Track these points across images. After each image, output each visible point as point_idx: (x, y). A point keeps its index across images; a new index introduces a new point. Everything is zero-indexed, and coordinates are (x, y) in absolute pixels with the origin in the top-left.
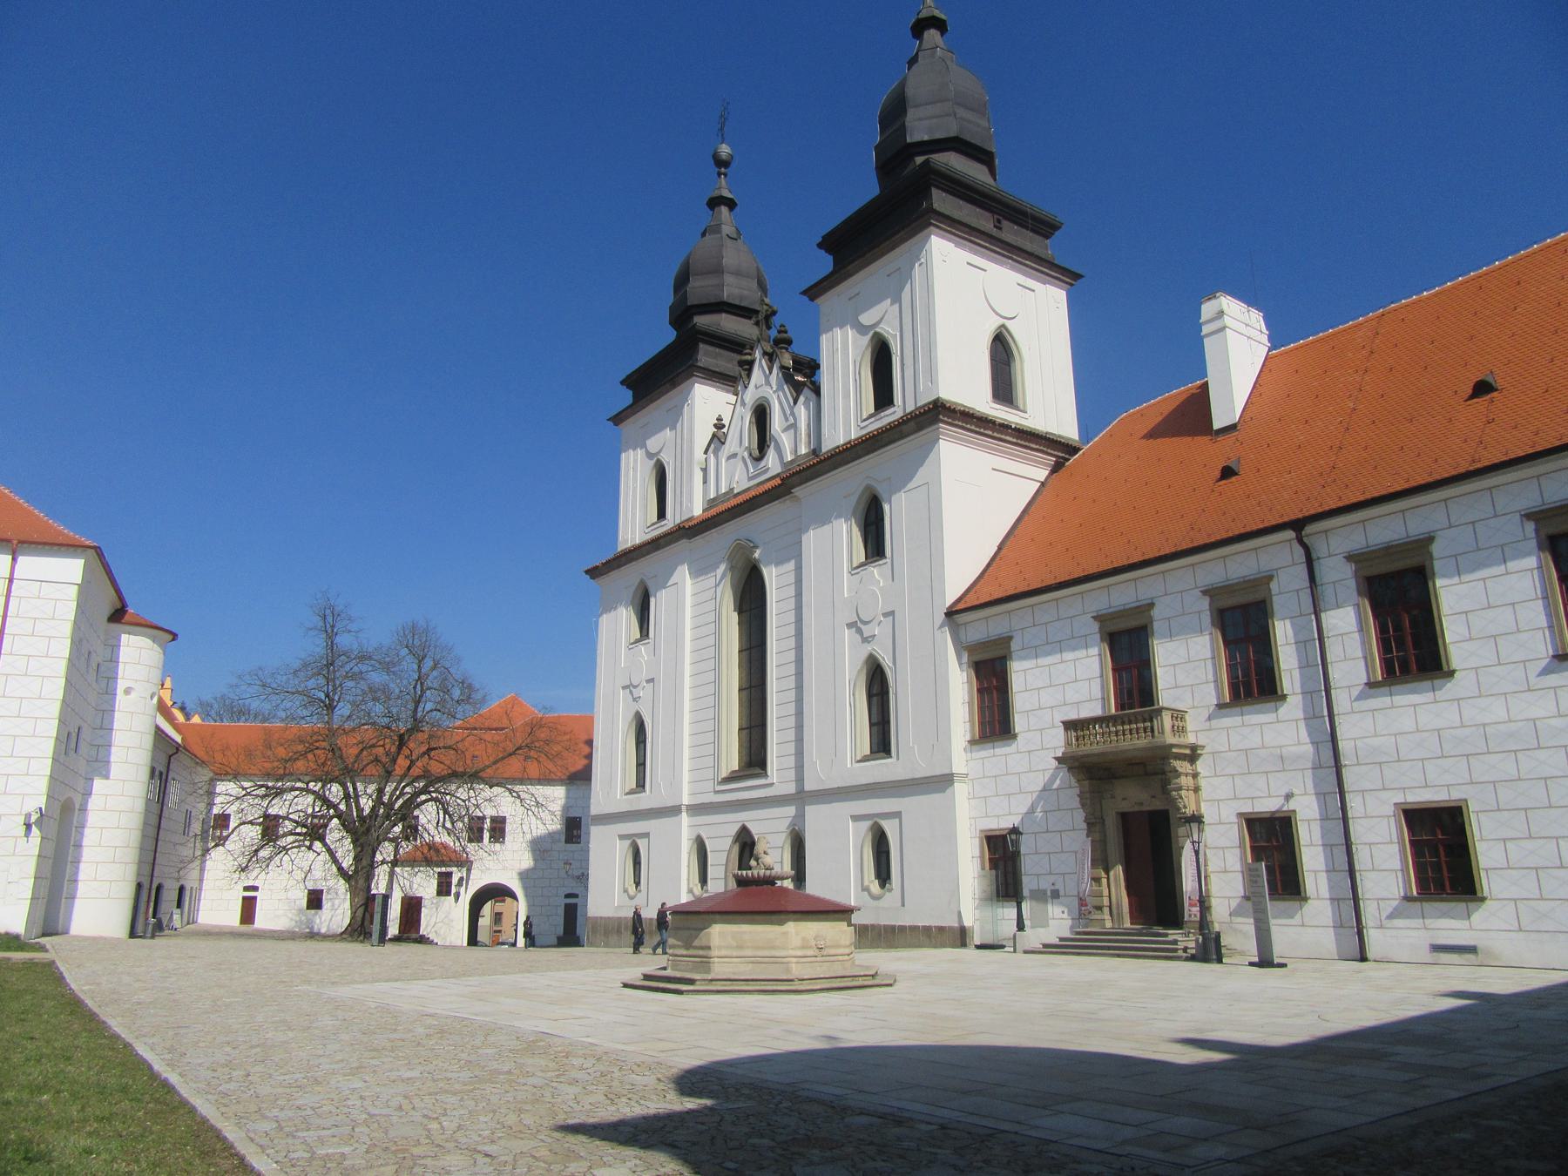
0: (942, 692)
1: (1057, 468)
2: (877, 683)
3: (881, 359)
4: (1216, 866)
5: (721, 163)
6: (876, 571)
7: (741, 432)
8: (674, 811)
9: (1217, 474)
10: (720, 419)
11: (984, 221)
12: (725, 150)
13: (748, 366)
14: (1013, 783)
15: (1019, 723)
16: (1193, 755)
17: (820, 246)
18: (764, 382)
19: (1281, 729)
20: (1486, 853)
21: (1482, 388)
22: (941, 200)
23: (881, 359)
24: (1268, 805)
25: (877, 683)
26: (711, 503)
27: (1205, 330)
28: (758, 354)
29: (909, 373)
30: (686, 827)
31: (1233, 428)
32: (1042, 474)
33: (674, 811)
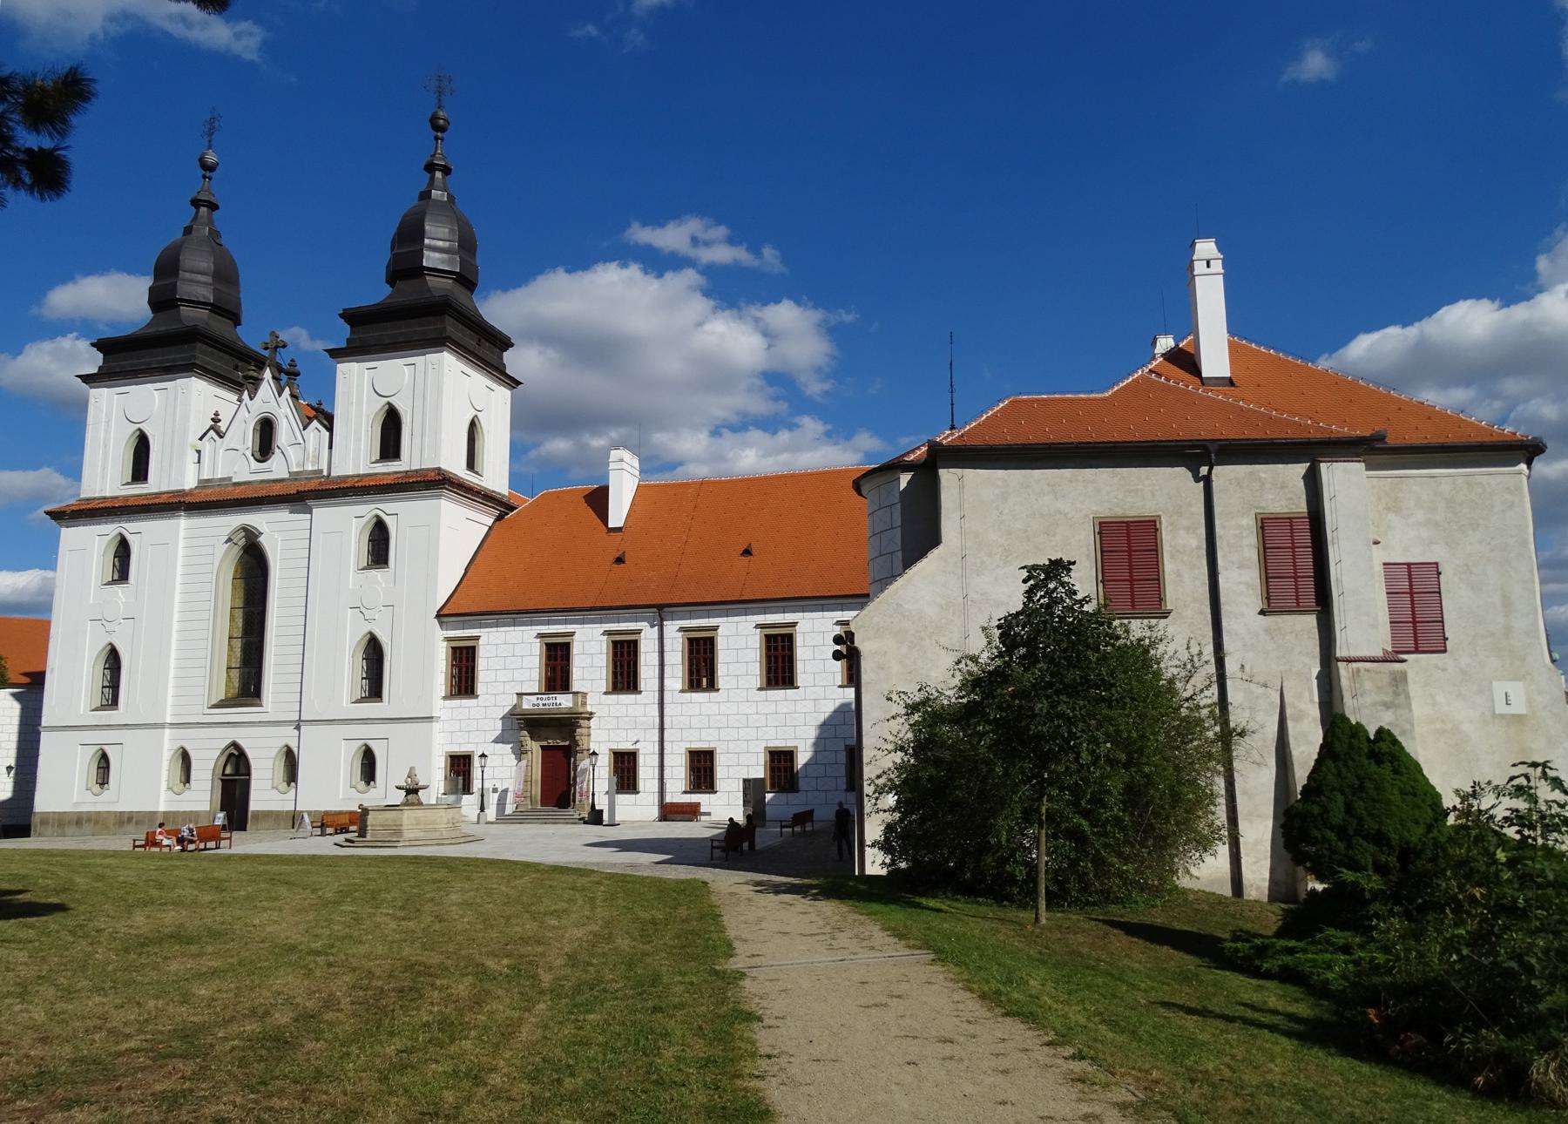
0: (420, 660)
1: (499, 518)
2: (374, 653)
3: (391, 425)
4: (597, 779)
5: (208, 168)
6: (377, 574)
7: (243, 435)
8: (161, 726)
9: (612, 559)
10: (216, 414)
11: (471, 343)
12: (211, 158)
13: (256, 382)
14: (475, 725)
15: (480, 688)
16: (590, 717)
17: (341, 316)
18: (269, 399)
19: (640, 706)
20: (720, 772)
21: (747, 552)
22: (451, 327)
23: (391, 425)
24: (626, 746)
25: (374, 653)
26: (204, 484)
27: (611, 466)
28: (268, 374)
29: (417, 441)
30: (168, 743)
31: (619, 530)
32: (490, 521)
33: (161, 726)
